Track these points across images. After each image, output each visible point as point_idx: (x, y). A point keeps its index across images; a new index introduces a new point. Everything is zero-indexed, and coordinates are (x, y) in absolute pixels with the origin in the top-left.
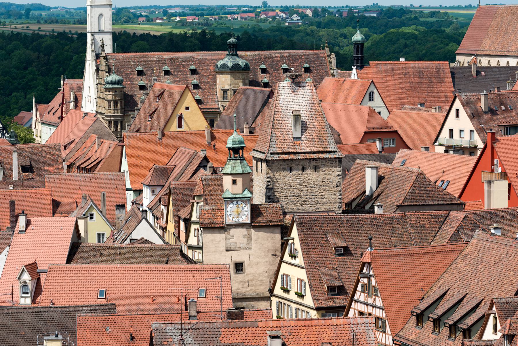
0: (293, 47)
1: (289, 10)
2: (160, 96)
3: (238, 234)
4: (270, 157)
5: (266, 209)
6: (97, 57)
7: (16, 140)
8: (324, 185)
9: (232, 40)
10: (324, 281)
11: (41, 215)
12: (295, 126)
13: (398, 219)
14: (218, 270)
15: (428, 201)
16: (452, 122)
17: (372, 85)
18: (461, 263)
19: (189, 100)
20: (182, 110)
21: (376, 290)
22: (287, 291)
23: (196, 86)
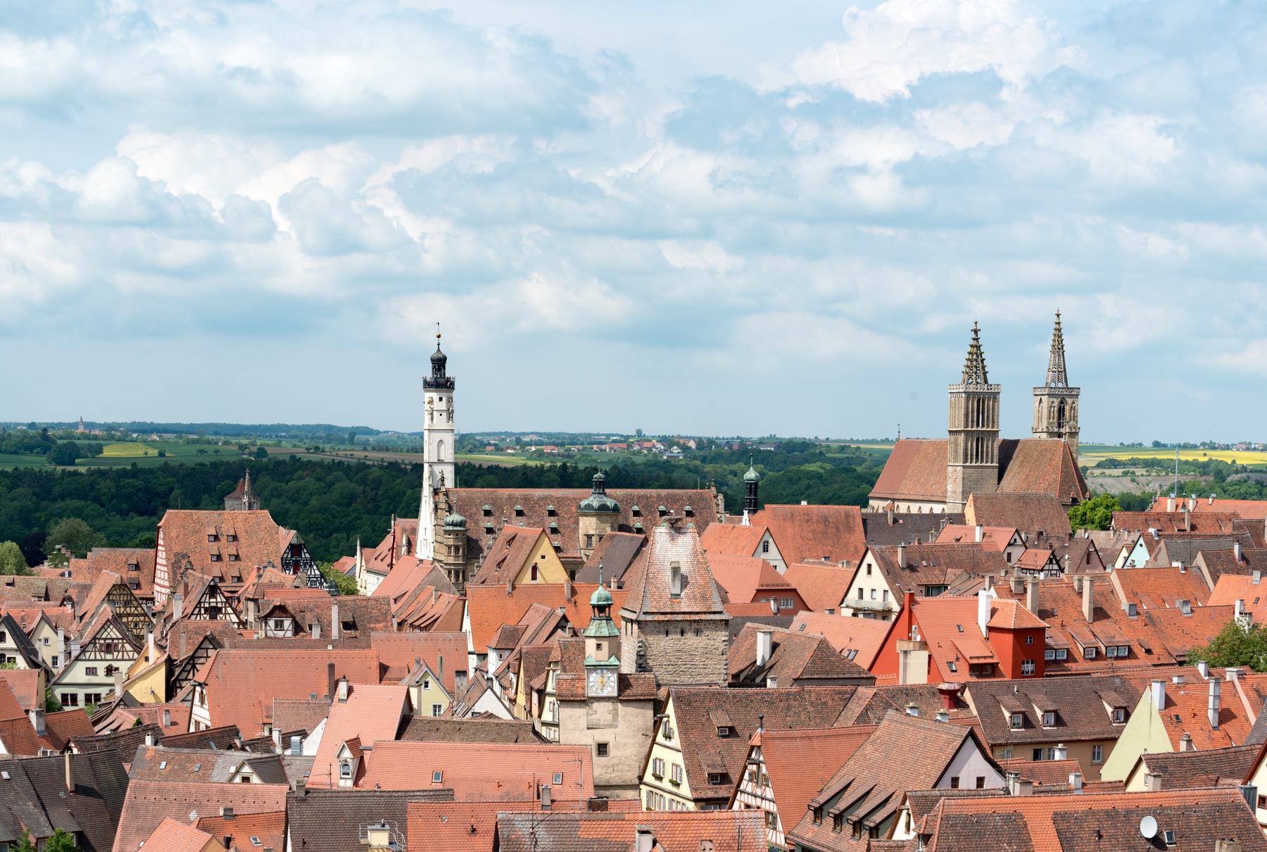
0: (671, 485)
1: (668, 442)
2: (510, 542)
3: (602, 711)
4: (643, 618)
5: (636, 679)
6: (436, 492)
7: (336, 590)
8: (707, 653)
9: (599, 474)
10: (704, 767)
12: (673, 580)
13: (794, 694)
14: (577, 752)
15: (832, 675)
16: (862, 580)
17: (767, 534)
18: (869, 748)
19: (546, 547)
20: (537, 559)
21: (766, 780)
22: (659, 778)
23: (554, 531)
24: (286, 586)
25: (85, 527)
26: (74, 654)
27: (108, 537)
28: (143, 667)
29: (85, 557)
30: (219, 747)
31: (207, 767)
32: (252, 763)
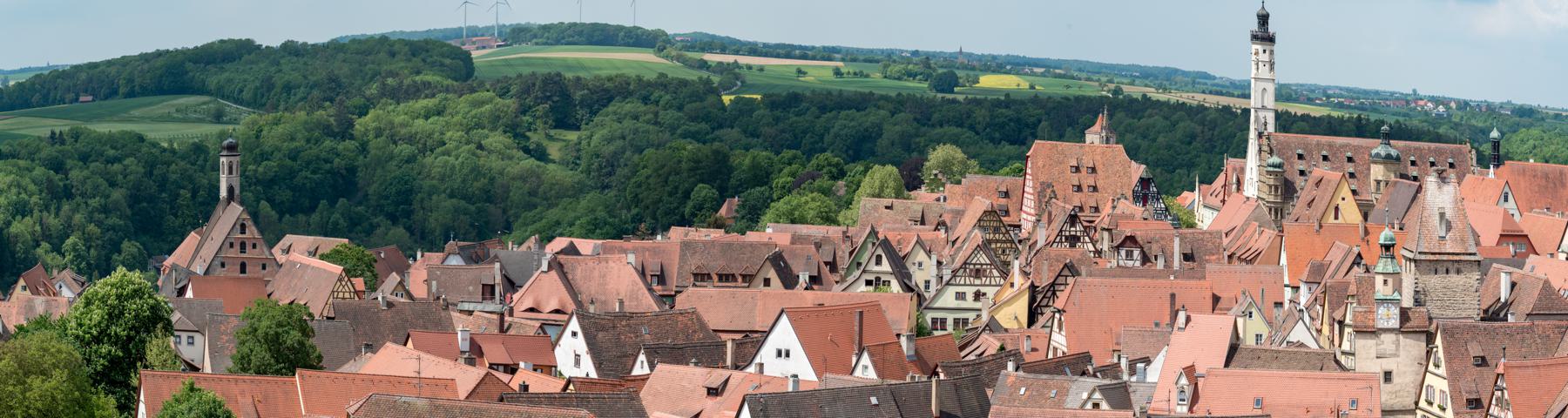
0: (1438, 139)
1: (1437, 101)
2: (1318, 184)
3: (1388, 339)
4: (1419, 257)
7: (1178, 223)
9: (1385, 128)
11: (1201, 312)
14: (1368, 377)
19: (1345, 191)
22: (1430, 404)
23: (1352, 175)
24: (1136, 217)
25: (959, 154)
26: (946, 278)
27: (981, 165)
28: (1009, 293)
29: (959, 182)
30: (1074, 373)
31: (1063, 393)
32: (1102, 389)
